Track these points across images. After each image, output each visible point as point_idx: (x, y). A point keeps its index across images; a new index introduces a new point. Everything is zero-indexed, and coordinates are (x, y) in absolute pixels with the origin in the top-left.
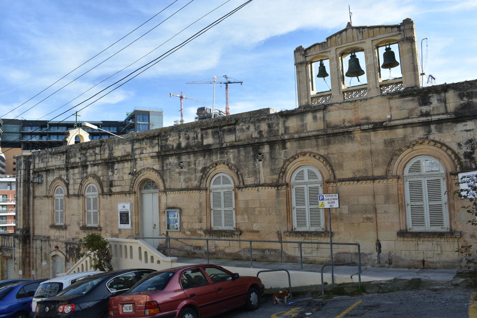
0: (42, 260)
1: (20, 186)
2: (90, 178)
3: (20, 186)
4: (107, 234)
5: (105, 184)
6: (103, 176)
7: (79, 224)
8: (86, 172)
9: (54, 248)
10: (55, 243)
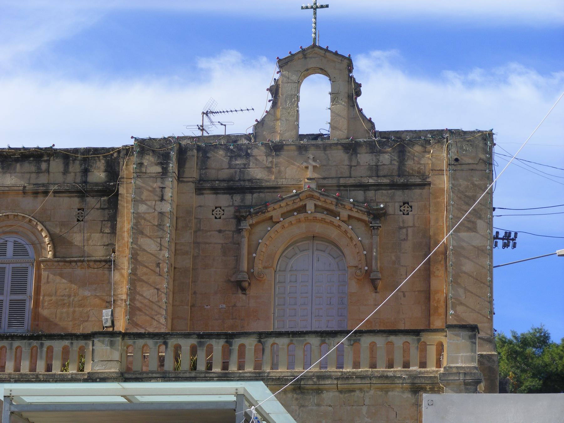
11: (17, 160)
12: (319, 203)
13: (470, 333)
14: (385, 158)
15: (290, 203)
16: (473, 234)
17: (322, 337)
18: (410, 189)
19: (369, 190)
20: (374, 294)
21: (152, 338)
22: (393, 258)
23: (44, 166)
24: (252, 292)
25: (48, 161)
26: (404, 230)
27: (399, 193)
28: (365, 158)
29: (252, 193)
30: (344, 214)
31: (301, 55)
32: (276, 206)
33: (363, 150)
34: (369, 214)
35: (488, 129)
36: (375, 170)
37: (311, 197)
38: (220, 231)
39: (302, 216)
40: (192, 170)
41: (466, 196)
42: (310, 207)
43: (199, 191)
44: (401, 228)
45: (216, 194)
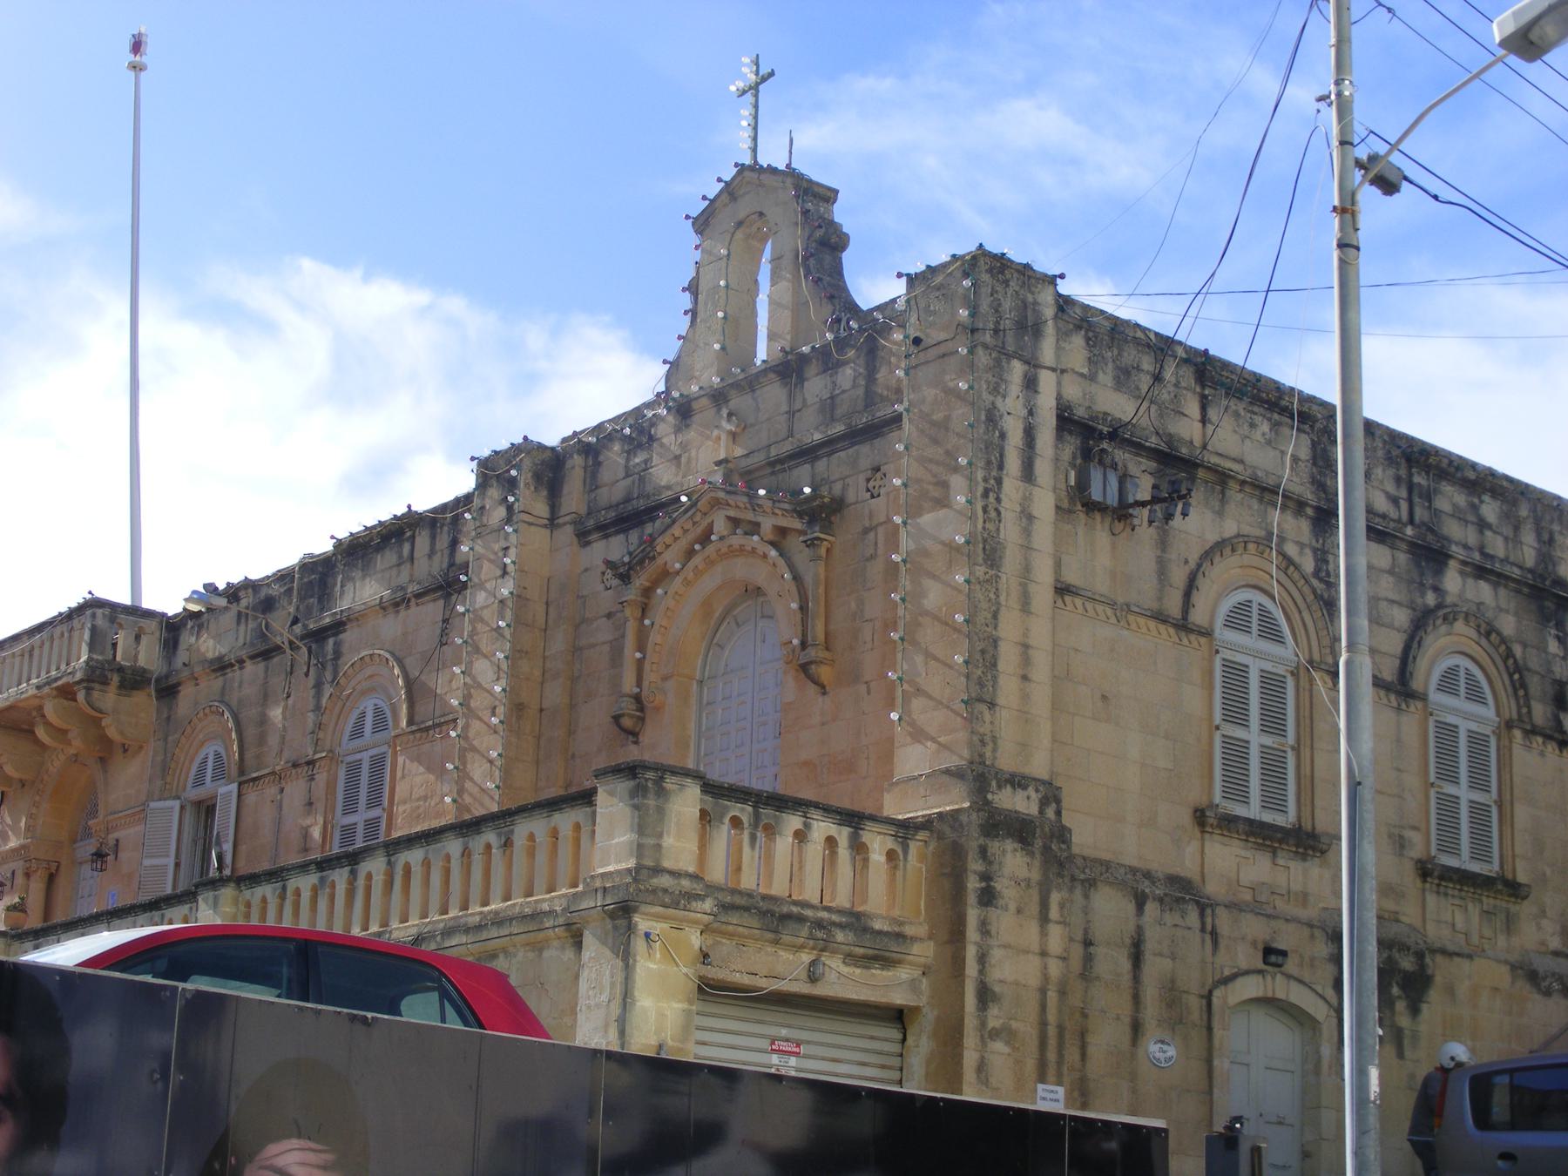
0: (1136, 1028)
1: (1028, 474)
2: (1459, 626)
3: (1028, 474)
4: (1545, 922)
5: (1534, 684)
6: (1525, 646)
7: (1400, 844)
8: (1436, 589)
9: (1246, 957)
10: (1255, 928)
11: (379, 548)
12: (732, 513)
13: (631, 784)
14: (846, 376)
15: (688, 526)
16: (942, 513)
17: (463, 836)
18: (877, 436)
19: (817, 458)
20: (820, 699)
21: (268, 881)
22: (853, 605)
23: (406, 548)
24: (645, 739)
25: (413, 537)
26: (871, 535)
27: (864, 449)
28: (816, 386)
29: (653, 520)
30: (767, 524)
31: (725, 197)
32: (667, 538)
33: (812, 369)
34: (800, 515)
35: (973, 248)
36: (829, 407)
37: (716, 504)
38: (609, 616)
39: (710, 549)
40: (573, 499)
41: (934, 424)
42: (721, 526)
43: (583, 537)
44: (866, 531)
45: (606, 537)
